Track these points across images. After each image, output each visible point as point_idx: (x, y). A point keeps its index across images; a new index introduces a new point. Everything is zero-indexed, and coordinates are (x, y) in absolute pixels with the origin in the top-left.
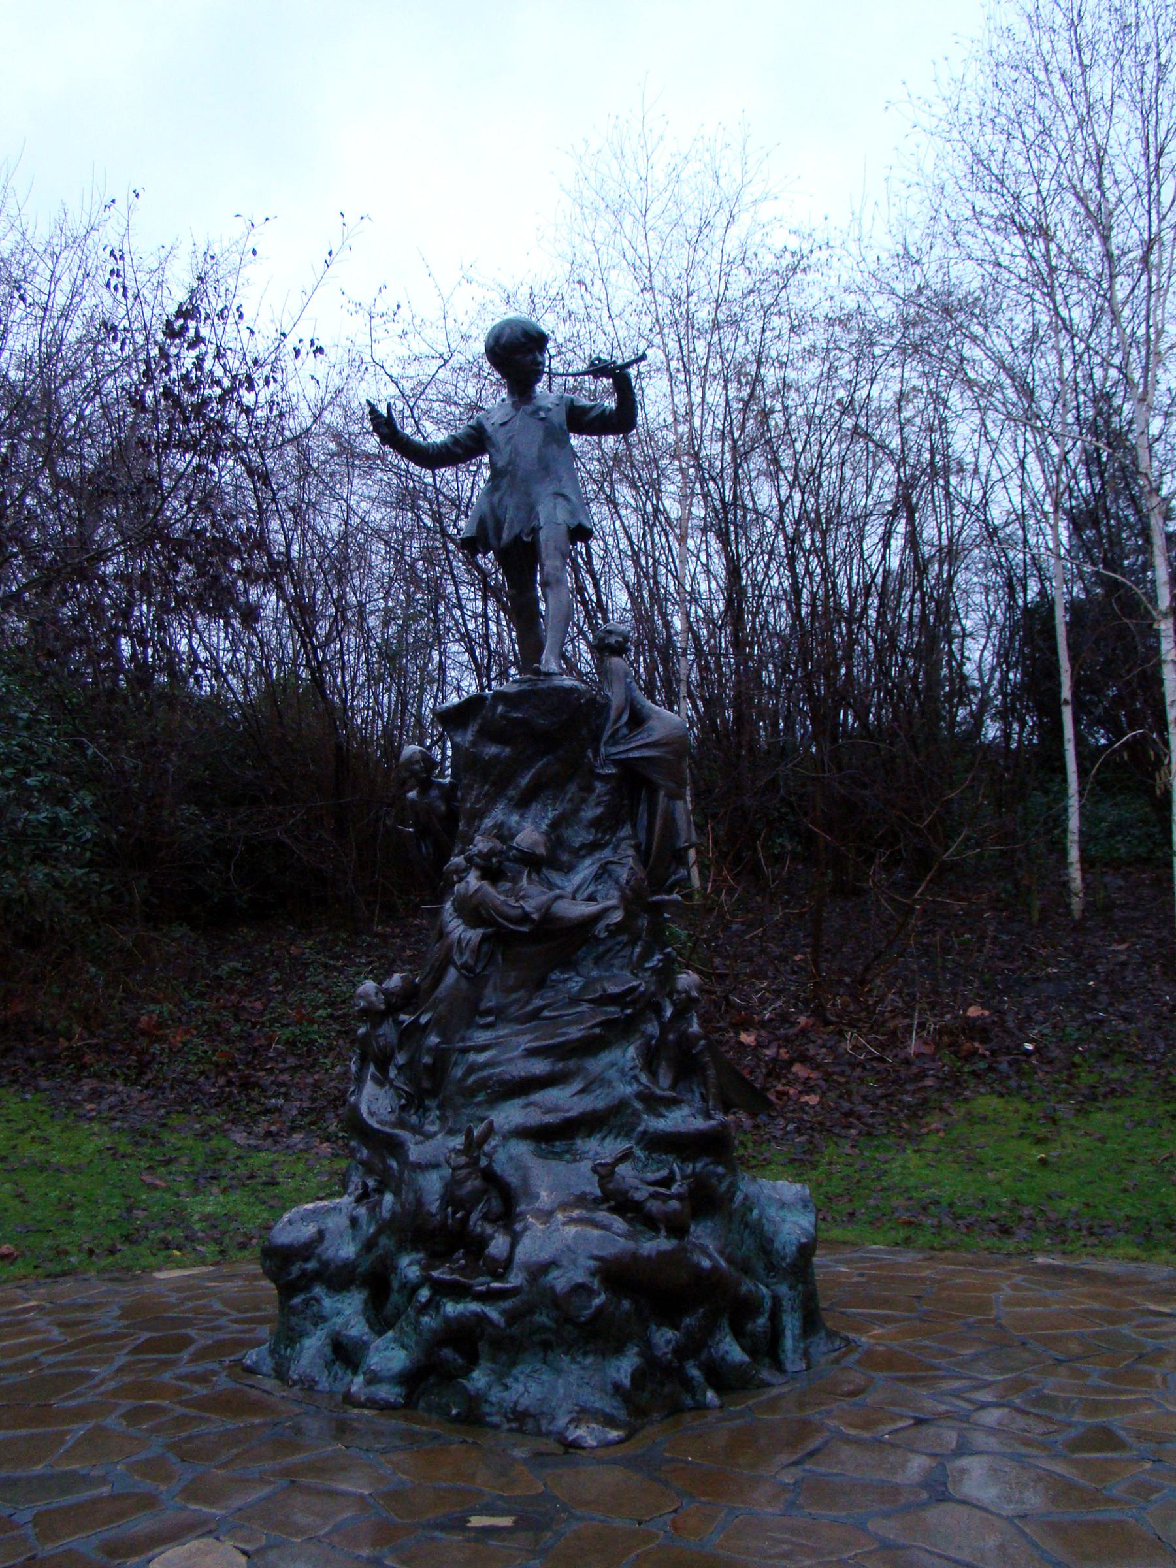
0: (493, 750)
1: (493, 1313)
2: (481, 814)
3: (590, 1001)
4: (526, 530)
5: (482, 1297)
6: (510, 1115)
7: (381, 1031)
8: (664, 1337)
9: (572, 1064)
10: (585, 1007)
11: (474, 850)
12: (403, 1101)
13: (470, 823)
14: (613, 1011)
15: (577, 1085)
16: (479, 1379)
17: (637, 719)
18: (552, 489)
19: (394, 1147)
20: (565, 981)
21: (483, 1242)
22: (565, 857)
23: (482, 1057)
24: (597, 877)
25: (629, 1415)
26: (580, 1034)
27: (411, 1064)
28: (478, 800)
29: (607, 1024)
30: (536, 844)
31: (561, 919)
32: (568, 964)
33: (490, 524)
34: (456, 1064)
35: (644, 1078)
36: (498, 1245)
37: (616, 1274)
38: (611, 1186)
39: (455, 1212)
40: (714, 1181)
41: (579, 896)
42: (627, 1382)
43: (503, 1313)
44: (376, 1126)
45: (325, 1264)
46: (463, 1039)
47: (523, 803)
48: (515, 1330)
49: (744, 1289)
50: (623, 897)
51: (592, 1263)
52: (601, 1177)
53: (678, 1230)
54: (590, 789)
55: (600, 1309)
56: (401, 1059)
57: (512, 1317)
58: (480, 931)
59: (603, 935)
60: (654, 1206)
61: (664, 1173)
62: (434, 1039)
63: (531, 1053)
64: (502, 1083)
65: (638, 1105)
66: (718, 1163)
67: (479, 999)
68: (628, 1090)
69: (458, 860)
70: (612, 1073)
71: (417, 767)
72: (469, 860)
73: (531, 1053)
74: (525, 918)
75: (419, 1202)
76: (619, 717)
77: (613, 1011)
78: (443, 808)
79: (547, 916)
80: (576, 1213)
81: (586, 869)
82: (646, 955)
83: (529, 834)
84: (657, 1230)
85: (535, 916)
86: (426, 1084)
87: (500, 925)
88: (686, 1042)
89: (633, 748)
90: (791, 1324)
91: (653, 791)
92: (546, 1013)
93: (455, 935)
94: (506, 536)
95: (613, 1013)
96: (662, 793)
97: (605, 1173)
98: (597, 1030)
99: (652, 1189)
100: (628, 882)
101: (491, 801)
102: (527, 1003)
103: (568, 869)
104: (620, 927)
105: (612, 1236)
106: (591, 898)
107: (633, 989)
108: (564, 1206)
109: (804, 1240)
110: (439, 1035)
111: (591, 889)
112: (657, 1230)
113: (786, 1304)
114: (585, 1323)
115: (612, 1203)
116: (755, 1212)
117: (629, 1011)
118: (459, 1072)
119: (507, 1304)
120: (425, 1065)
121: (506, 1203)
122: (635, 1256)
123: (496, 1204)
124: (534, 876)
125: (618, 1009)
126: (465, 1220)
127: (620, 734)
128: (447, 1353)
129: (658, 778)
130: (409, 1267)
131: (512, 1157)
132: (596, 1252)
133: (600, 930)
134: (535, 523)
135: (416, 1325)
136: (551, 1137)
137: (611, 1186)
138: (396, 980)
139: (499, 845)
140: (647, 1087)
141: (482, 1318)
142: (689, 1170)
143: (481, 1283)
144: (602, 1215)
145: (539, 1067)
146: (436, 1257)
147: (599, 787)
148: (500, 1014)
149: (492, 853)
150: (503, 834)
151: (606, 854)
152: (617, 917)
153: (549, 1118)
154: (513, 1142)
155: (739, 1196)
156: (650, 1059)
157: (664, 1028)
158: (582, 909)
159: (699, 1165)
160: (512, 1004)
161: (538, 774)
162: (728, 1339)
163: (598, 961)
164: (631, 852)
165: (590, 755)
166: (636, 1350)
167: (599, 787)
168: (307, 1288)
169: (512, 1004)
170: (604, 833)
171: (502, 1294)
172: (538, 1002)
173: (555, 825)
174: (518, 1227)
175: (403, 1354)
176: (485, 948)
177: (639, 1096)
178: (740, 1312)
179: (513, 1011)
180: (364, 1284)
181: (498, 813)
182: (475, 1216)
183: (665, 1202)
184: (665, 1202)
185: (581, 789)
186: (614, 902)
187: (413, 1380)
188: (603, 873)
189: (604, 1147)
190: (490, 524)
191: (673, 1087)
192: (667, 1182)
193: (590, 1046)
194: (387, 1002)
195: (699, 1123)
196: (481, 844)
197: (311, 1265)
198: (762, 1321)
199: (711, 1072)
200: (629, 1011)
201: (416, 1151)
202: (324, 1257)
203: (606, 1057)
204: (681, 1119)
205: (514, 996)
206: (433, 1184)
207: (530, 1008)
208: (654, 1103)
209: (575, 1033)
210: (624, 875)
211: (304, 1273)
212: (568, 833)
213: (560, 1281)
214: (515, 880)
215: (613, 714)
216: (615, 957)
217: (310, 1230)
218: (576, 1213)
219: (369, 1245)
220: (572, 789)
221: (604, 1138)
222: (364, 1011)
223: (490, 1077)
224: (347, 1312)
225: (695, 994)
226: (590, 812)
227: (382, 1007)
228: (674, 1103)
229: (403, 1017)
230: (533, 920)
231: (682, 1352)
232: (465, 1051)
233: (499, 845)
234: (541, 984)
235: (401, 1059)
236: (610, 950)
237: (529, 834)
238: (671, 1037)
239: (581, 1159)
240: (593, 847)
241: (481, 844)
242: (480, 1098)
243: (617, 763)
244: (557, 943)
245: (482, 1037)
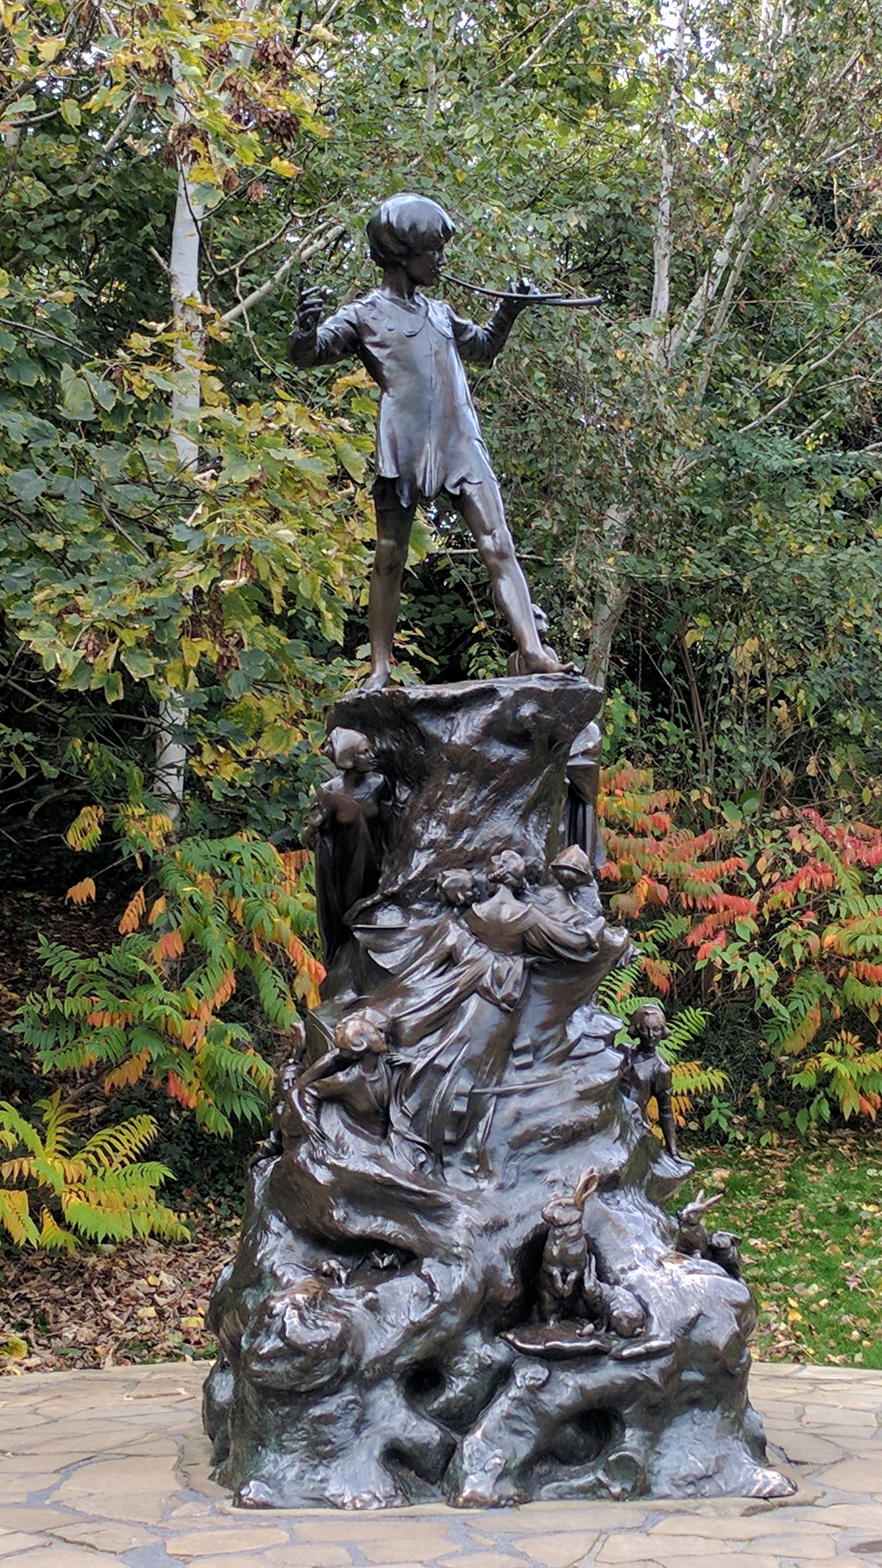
2: (476, 824)
5: (623, 1361)
36: (623, 1304)
39: (564, 1274)
57: (668, 1375)
62: (465, 1084)
86: (448, 1136)
101: (492, 806)
119: (662, 1363)
120: (456, 1114)
126: (580, 1281)
160: (547, 1042)
169: (547, 1042)
171: (651, 1355)
187: (528, 1465)
197: (345, 1362)
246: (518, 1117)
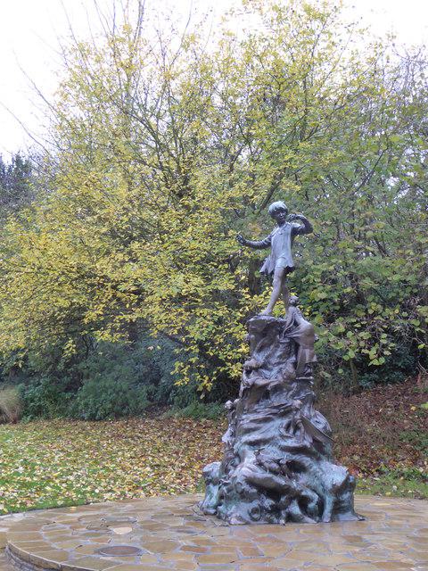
14: (275, 411)
24: (278, 372)
60: (266, 465)
63: (251, 421)
77: (275, 411)
81: (276, 369)
103: (271, 370)
122: (255, 478)
145: (253, 425)
148: (249, 412)
179: (251, 410)
193: (266, 420)
209: (260, 416)
215: (288, 323)
220: (272, 347)
226: (278, 353)
240: (279, 363)
245: (244, 417)
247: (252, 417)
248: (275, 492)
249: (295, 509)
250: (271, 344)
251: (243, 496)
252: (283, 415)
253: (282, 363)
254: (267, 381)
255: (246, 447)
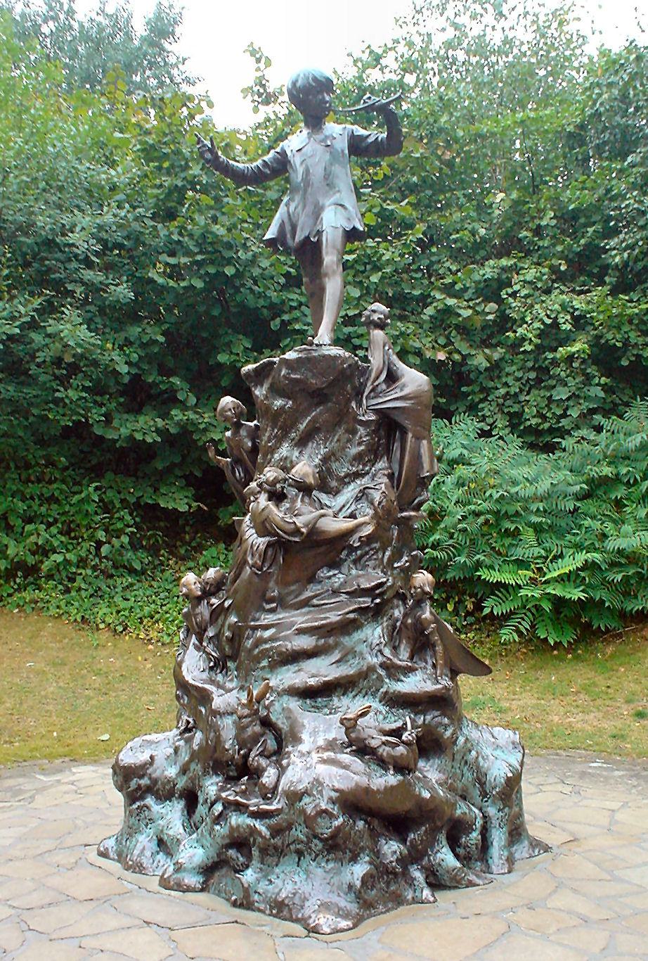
0: (279, 403)
1: (260, 826)
2: (273, 450)
3: (347, 593)
4: (314, 233)
6: (290, 677)
7: (198, 610)
8: (391, 849)
9: (331, 641)
10: (343, 597)
11: (263, 478)
12: (212, 664)
13: (265, 456)
14: (366, 601)
15: (336, 656)
16: (249, 876)
17: (392, 378)
18: (332, 200)
19: (205, 697)
20: (329, 578)
21: (256, 773)
22: (334, 484)
23: (267, 634)
24: (357, 499)
25: (360, 908)
26: (339, 618)
27: (218, 636)
28: (269, 441)
29: (361, 611)
30: (306, 475)
31: (324, 532)
32: (335, 564)
33: (288, 228)
34: (248, 638)
35: (387, 652)
36: (269, 777)
37: (354, 803)
38: (353, 735)
40: (441, 729)
41: (341, 515)
42: (358, 884)
43: (268, 827)
44: (191, 681)
45: (155, 781)
46: (254, 620)
47: (302, 443)
48: (277, 841)
49: (458, 812)
50: (376, 515)
51: (334, 795)
52: (347, 729)
53: (402, 768)
54: (354, 432)
55: (338, 829)
56: (210, 633)
58: (267, 539)
59: (356, 545)
60: (385, 751)
61: (399, 724)
62: (233, 619)
63: (301, 632)
64: (280, 654)
65: (383, 673)
66: (444, 714)
67: (265, 591)
68: (375, 661)
69: (253, 485)
70: (363, 648)
71: (229, 413)
72: (260, 485)
73: (301, 632)
74: (297, 531)
75: (218, 737)
76: (377, 378)
77: (366, 601)
78: (250, 444)
79: (313, 530)
80: (326, 755)
82: (397, 556)
83: (305, 467)
84: (386, 769)
85: (304, 530)
87: (278, 535)
88: (419, 627)
89: (390, 400)
90: (498, 837)
91: (404, 432)
92: (315, 602)
93: (250, 541)
94: (300, 236)
95: (364, 602)
96: (410, 435)
97: (350, 725)
98: (352, 616)
99: (384, 738)
100: (380, 503)
101: (280, 440)
102: (300, 594)
103: (335, 492)
104: (370, 539)
105: (351, 774)
106: (353, 516)
107: (380, 585)
108: (319, 749)
109: (510, 775)
110: (238, 616)
111: (353, 507)
112: (386, 769)
113: (495, 822)
114: (327, 839)
115: (354, 748)
116: (473, 753)
117: (378, 601)
118: (249, 643)
119: (273, 821)
121: (281, 740)
122: (367, 790)
123: (271, 744)
124: (306, 499)
125: (369, 600)
126: (246, 756)
127: (379, 389)
128: (232, 853)
129: (407, 423)
130: (211, 786)
131: (282, 709)
132: (337, 785)
133: (354, 541)
134: (319, 228)
135: (211, 831)
136: (314, 694)
137: (353, 735)
138: (211, 573)
139: (282, 475)
140: (388, 659)
141: (253, 831)
142: (420, 720)
143: (254, 803)
144: (346, 758)
145: (306, 642)
146: (231, 780)
147: (362, 431)
149: (276, 481)
150: (286, 466)
151: (365, 481)
152: (368, 530)
153: (312, 682)
154: (286, 698)
155: (461, 740)
156: (394, 635)
157: (406, 615)
158: (343, 524)
159: (429, 718)
161: (314, 421)
162: (444, 850)
163: (355, 562)
164: (386, 480)
165: (353, 405)
166: (367, 859)
167: (362, 431)
168: (142, 798)
170: (365, 465)
172: (308, 594)
173: (325, 460)
174: (284, 762)
175: (200, 851)
176: (269, 553)
177: (382, 665)
178: (455, 831)
180: (180, 797)
181: (285, 450)
182: (252, 754)
183: (393, 748)
184: (393, 748)
185: (347, 431)
186: (367, 519)
187: (208, 870)
188: (363, 495)
189: (350, 705)
190: (288, 228)
191: (411, 658)
192: (397, 733)
193: (347, 627)
194: (203, 590)
195: (430, 687)
196: (270, 473)
197: (145, 782)
198: (475, 835)
199: (439, 648)
200: (378, 601)
201: (218, 702)
202: (154, 776)
203: (358, 635)
204: (416, 683)
205: (293, 588)
206: (228, 728)
207: (303, 597)
208: (393, 670)
209: (334, 617)
210: (377, 496)
211: (139, 787)
212: (334, 466)
213: (308, 804)
214: (293, 501)
215: (373, 375)
216: (370, 559)
217: (145, 757)
218: (326, 755)
219: (184, 770)
220: (341, 431)
221: (354, 697)
222: (187, 596)
223: (272, 648)
224: (171, 815)
225: (427, 589)
226: (354, 450)
227: (200, 593)
228: (409, 670)
229: (213, 600)
230: (303, 533)
231: (405, 862)
232: (255, 628)
233: (282, 475)
234: (312, 579)
235: (210, 633)
236: (367, 553)
237: (305, 467)
238: (409, 621)
239: (335, 713)
240: (358, 475)
241: (270, 473)
242: (264, 663)
243: (376, 411)
244: (328, 549)
245: (267, 619)
246: (256, 645)
247: (301, 619)
248: (397, 822)
249: (445, 857)
250: (338, 424)
251: (336, 848)
252: (376, 613)
253: (363, 476)
254: (351, 523)
255: (294, 704)
